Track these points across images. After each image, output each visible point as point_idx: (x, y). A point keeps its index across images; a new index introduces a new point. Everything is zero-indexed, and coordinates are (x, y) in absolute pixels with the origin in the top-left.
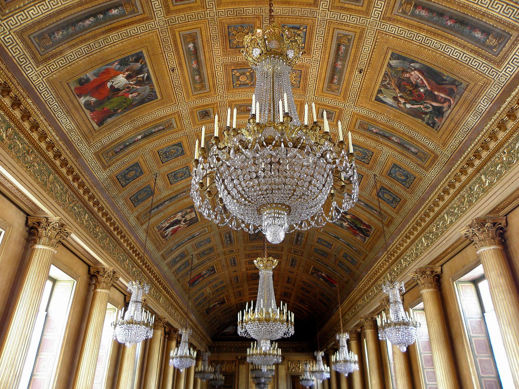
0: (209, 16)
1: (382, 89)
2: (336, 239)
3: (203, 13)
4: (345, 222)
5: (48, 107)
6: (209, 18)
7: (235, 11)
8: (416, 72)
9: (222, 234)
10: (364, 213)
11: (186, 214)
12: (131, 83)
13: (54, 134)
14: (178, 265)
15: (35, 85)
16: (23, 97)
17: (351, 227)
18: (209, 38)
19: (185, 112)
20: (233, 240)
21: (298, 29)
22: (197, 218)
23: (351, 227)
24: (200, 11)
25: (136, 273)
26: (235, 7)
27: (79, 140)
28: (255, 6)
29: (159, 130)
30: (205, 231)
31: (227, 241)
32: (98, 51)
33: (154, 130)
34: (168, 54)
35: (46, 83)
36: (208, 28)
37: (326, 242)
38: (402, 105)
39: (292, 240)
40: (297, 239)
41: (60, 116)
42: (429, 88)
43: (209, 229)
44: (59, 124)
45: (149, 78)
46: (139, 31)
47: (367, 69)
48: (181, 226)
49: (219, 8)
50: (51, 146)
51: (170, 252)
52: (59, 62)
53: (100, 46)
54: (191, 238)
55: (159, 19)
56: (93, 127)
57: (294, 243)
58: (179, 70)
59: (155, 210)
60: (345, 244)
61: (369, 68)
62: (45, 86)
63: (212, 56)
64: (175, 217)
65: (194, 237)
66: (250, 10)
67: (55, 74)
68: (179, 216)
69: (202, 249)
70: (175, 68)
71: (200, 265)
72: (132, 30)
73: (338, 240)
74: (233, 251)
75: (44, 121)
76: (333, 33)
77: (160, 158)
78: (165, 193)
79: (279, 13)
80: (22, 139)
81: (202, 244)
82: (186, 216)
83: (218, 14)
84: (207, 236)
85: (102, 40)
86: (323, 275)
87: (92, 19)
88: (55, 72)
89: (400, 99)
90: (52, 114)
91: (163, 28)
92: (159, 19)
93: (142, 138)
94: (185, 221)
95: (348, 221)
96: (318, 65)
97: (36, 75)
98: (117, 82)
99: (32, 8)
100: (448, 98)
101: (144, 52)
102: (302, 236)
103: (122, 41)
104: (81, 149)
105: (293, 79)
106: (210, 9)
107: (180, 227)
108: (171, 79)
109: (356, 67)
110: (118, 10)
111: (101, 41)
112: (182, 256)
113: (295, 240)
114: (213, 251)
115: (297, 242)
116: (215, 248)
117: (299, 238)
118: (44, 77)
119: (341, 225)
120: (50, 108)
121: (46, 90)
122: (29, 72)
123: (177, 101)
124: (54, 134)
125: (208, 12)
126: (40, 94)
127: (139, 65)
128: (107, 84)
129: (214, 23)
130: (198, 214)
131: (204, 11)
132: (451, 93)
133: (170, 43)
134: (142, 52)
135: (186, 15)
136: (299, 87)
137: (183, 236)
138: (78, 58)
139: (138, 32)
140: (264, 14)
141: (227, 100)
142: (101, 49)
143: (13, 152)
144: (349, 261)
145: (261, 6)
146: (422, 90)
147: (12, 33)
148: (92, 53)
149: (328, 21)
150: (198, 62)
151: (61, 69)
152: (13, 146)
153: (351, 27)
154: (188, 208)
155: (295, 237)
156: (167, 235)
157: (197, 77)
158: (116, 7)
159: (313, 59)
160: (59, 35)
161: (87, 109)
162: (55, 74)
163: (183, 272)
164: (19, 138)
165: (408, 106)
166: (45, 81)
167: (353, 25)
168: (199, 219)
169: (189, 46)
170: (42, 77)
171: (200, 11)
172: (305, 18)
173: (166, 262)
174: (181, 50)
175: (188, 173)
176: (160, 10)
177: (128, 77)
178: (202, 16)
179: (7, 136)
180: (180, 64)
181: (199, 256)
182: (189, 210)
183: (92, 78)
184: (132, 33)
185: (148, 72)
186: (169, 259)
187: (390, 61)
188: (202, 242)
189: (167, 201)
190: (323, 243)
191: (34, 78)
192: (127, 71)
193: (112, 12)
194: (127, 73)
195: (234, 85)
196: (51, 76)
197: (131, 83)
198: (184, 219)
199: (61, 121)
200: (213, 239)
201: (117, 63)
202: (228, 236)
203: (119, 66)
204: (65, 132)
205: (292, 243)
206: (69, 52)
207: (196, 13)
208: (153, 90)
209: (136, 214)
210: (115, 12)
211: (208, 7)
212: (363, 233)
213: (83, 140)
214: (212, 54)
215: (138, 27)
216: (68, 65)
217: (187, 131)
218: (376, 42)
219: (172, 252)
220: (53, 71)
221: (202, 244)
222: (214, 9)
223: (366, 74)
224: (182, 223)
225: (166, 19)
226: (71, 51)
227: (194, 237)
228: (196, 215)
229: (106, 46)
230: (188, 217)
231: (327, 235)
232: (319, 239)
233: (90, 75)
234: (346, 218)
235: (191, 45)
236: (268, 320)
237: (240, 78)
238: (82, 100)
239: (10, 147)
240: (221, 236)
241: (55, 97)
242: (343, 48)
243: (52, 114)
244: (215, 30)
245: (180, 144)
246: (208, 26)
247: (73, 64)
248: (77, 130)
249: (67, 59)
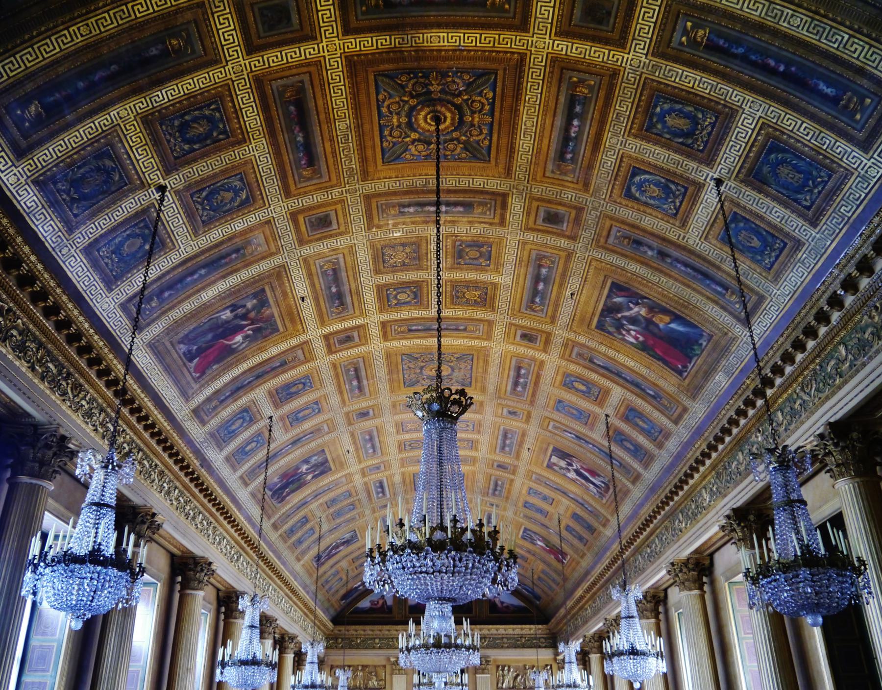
2: (295, 438)
4: (307, 470)
9: (529, 399)
10: (301, 497)
11: (561, 468)
14: (641, 440)
17: (296, 474)
20: (512, 373)
22: (553, 451)
23: (296, 474)
30: (555, 427)
31: (526, 376)
37: (305, 418)
39: (369, 372)
40: (358, 378)
43: (546, 424)
51: (624, 467)
57: (362, 365)
60: (278, 449)
65: (577, 436)
68: (572, 475)
69: (584, 404)
71: (618, 374)
73: (292, 441)
74: (524, 336)
78: (565, 501)
81: (575, 412)
82: (564, 466)
84: (556, 416)
86: (239, 338)
95: (305, 473)
102: (351, 390)
107: (582, 468)
113: (363, 373)
114: (569, 375)
115: (356, 370)
116: (559, 378)
117: (355, 383)
119: (306, 461)
137: (589, 455)
144: (248, 444)
154: (554, 470)
155: (365, 382)
156: (603, 482)
163: (656, 415)
168: (551, 448)
173: (640, 469)
181: (601, 397)
186: (636, 465)
188: (572, 414)
190: (307, 412)
198: (570, 468)
200: (552, 403)
202: (519, 389)
205: (367, 363)
209: (601, 528)
212: (280, 489)
219: (623, 463)
221: (575, 412)
227: (577, 436)
230: (563, 464)
231: (312, 430)
232: (319, 411)
234: (310, 473)
240: (534, 394)
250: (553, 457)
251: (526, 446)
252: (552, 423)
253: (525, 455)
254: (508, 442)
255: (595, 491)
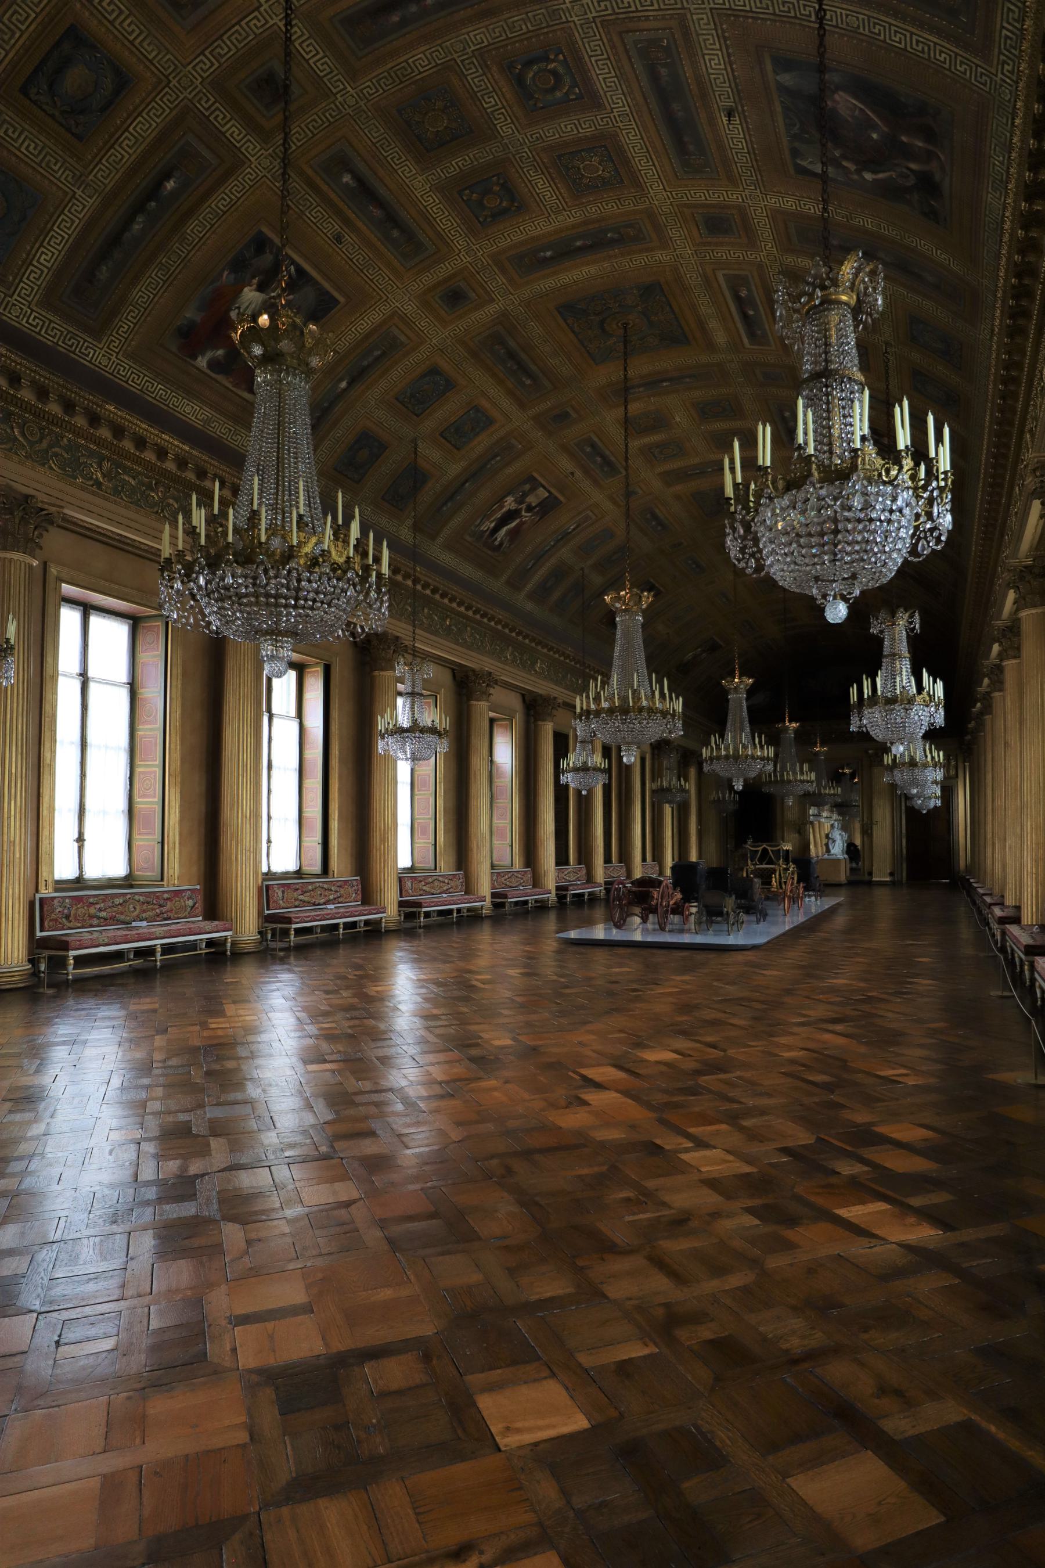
0: (346, 106)
1: (796, 144)
3: (332, 106)
5: (150, 399)
6: (349, 111)
7: (393, 74)
8: (841, 93)
11: (525, 495)
12: (273, 294)
13: (176, 443)
14: (556, 595)
15: (111, 371)
16: (98, 406)
18: (374, 148)
19: (410, 308)
21: (547, 60)
22: (556, 498)
24: (323, 105)
25: (453, 627)
26: (389, 66)
27: (230, 430)
28: (428, 47)
29: (378, 359)
32: (180, 267)
33: (365, 363)
34: (313, 213)
35: (126, 361)
36: (360, 131)
38: (855, 177)
41: (177, 405)
42: (886, 129)
44: (184, 418)
45: (300, 271)
46: (233, 197)
47: (742, 107)
48: (525, 522)
49: (358, 84)
50: (182, 463)
52: (129, 317)
53: (181, 256)
54: (562, 539)
55: (256, 157)
56: (244, 399)
58: (352, 235)
59: (449, 504)
61: (744, 102)
62: (128, 367)
63: (400, 181)
64: (502, 507)
66: (420, 58)
67: (132, 340)
68: (510, 503)
70: (340, 233)
72: (219, 202)
75: (150, 429)
76: (625, 46)
77: (407, 407)
78: (454, 469)
79: (485, 40)
80: (132, 469)
83: (361, 95)
85: (177, 245)
87: (140, 219)
88: (131, 336)
89: (845, 163)
90: (163, 406)
91: (274, 170)
92: (256, 157)
93: (349, 384)
94: (529, 509)
96: (633, 123)
97: (104, 356)
98: (247, 304)
99: (40, 251)
100: (931, 148)
101: (265, 230)
103: (213, 229)
104: (242, 445)
105: (598, 168)
106: (342, 93)
107: (522, 523)
108: (344, 257)
109: (715, 106)
110: (174, 179)
111: (177, 248)
112: (559, 573)
118: (118, 353)
120: (154, 398)
121: (132, 372)
122: (91, 355)
123: (381, 293)
124: (176, 443)
125: (340, 99)
126: (126, 383)
127: (268, 258)
128: (230, 317)
129: (365, 116)
130: (552, 490)
131: (333, 102)
132: (929, 134)
133: (303, 192)
134: (261, 232)
135: (302, 125)
136: (622, 181)
138: (155, 295)
139: (232, 200)
140: (455, 56)
141: (485, 255)
142: (185, 262)
143: (124, 498)
145: (439, 42)
146: (875, 136)
147: (35, 308)
148: (174, 275)
149: (598, 20)
150: (380, 204)
151: (137, 327)
152: (120, 489)
153: (654, 20)
156: (501, 544)
157: (395, 233)
158: (167, 176)
159: (616, 114)
160: (103, 273)
161: (218, 373)
162: (132, 340)
164: (127, 470)
165: (868, 176)
166: (123, 359)
167: (655, 13)
168: (562, 498)
169: (345, 180)
170: (115, 355)
171: (323, 105)
172: (545, 30)
174: (333, 196)
175: (484, 419)
176: (249, 140)
177: (261, 288)
178: (334, 114)
179: (104, 476)
180: (347, 222)
182: (527, 487)
183: (198, 318)
184: (222, 207)
185: (293, 262)
187: (778, 78)
189: (466, 481)
191: (105, 362)
192: (254, 277)
193: (166, 187)
194: (255, 281)
195: (481, 219)
196: (128, 346)
197: (273, 294)
198: (524, 506)
199: (184, 411)
201: (226, 273)
202: (649, 516)
203: (232, 276)
204: (199, 427)
206: (135, 293)
207: (320, 114)
208: (323, 293)
210: (170, 185)
211: (334, 91)
213: (237, 428)
214: (398, 177)
215: (227, 191)
216: (145, 315)
217: (434, 341)
218: (725, 41)
220: (126, 336)
222: (349, 89)
223: (745, 117)
224: (523, 513)
225: (270, 151)
226: (137, 290)
228: (549, 491)
229: (189, 252)
230: (532, 500)
233: (191, 314)
235: (347, 178)
236: (625, 710)
237: (485, 202)
238: (202, 362)
239: (116, 492)
241: (153, 377)
242: (664, 71)
243: (163, 406)
244: (375, 130)
245: (434, 371)
246: (357, 128)
247: (152, 309)
248: (218, 416)
249: (138, 306)
250: (547, 494)
251: (579, 474)
252: (594, 517)
253: (566, 464)
254: (599, 459)
255: (484, 528)
